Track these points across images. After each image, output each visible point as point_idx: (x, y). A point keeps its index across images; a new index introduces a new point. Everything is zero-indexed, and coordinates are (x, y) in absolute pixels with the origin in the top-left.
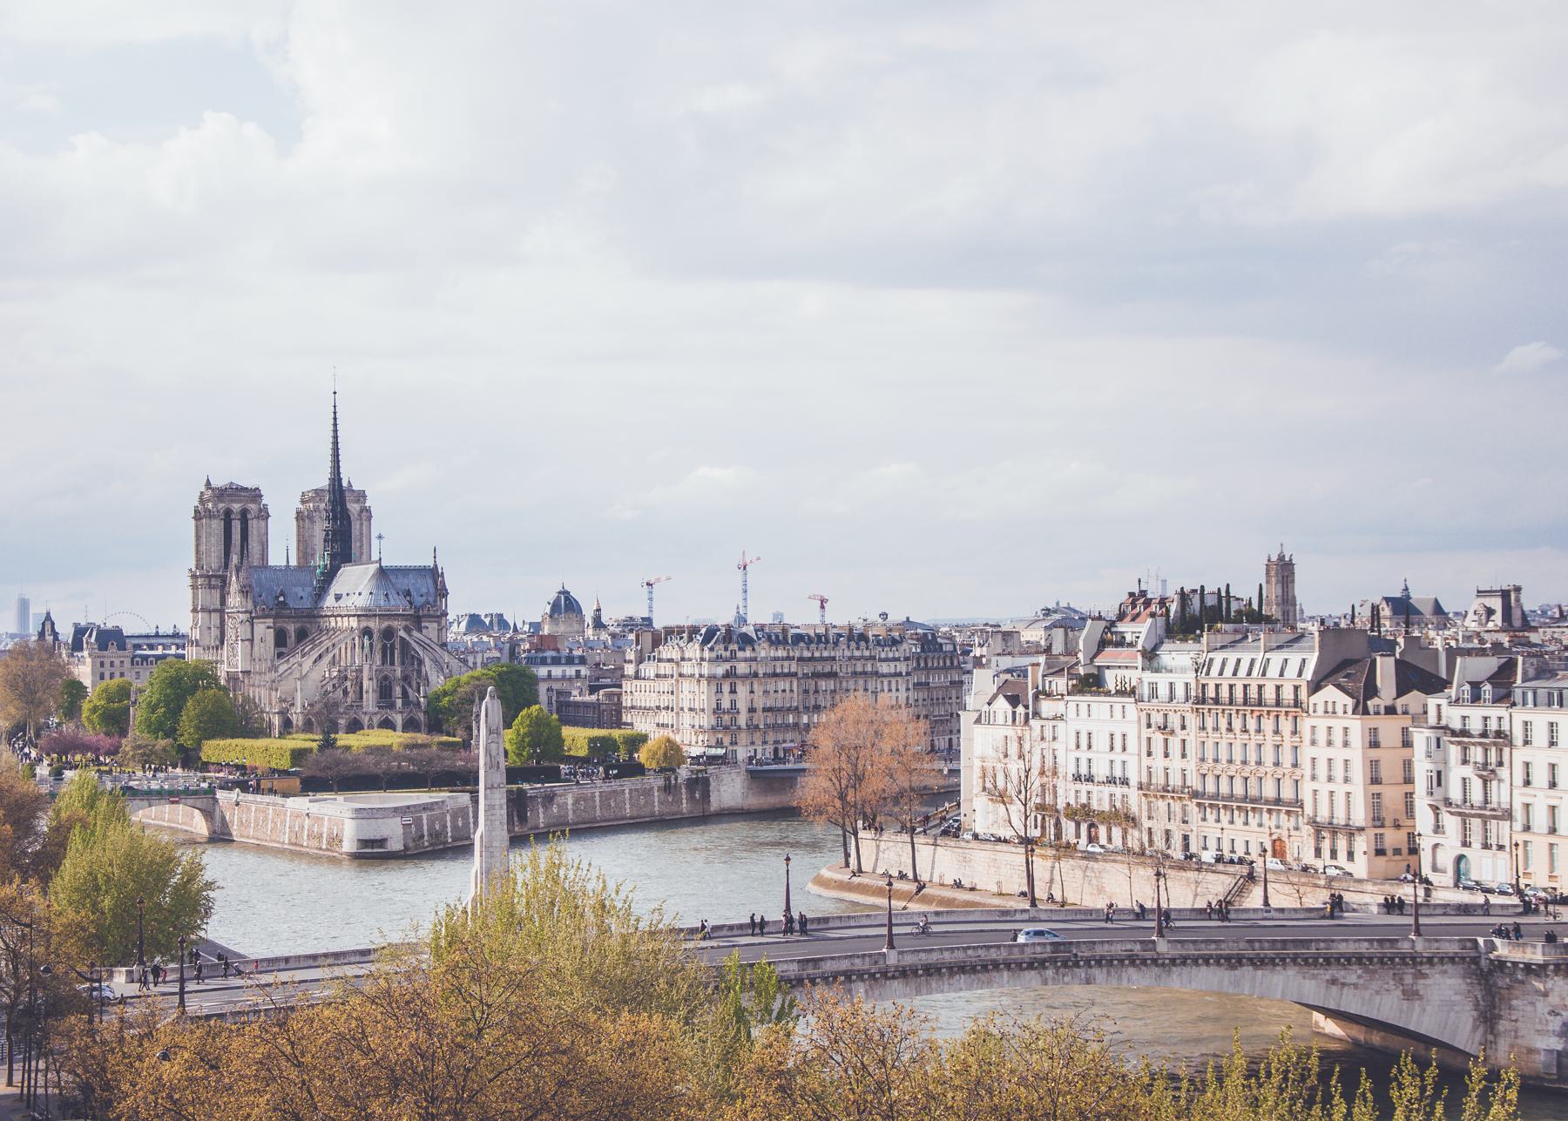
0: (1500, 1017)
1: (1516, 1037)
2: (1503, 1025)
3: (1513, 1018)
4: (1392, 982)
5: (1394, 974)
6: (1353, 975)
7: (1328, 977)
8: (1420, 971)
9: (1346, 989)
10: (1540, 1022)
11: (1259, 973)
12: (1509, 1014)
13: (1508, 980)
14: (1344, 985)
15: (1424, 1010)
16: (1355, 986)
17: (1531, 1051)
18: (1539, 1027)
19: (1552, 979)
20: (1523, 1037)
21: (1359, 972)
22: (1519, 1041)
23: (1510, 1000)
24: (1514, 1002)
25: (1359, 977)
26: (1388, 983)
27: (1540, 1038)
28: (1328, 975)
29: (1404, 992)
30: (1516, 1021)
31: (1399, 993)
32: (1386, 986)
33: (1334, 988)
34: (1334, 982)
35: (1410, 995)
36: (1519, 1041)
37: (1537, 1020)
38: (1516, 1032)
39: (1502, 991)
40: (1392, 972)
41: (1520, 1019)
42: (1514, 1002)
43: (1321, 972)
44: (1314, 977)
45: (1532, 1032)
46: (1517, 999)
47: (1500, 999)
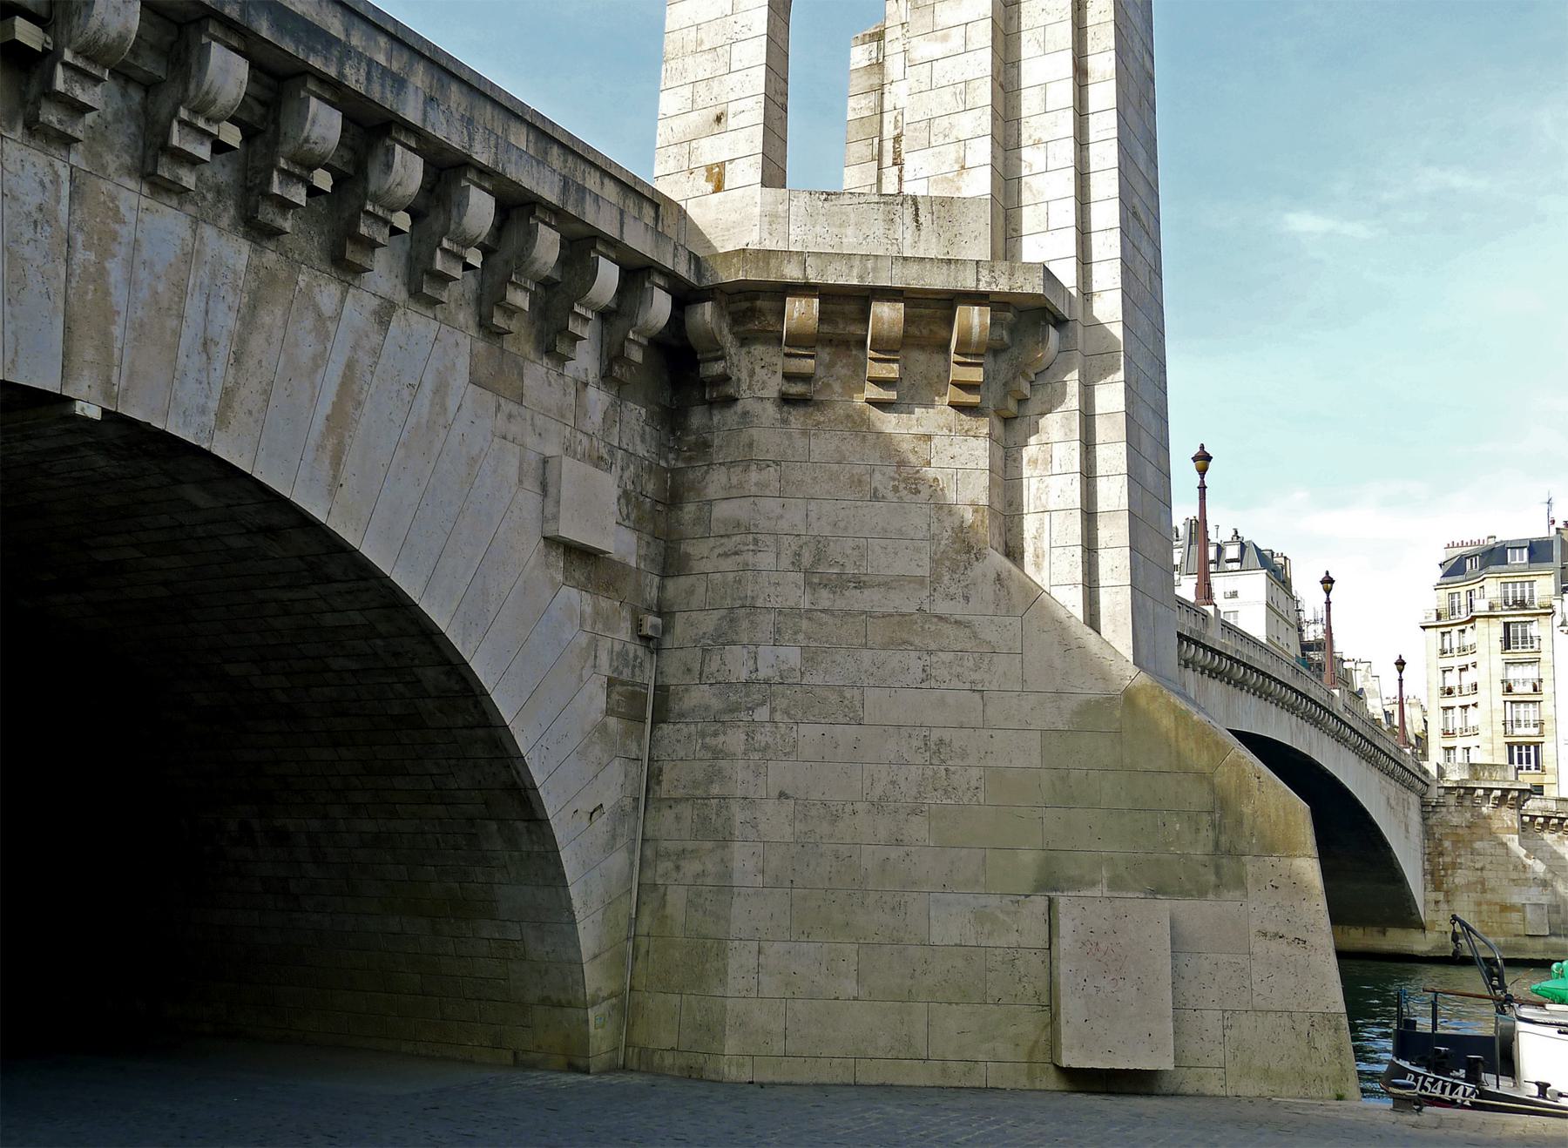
0: (1454, 866)
1: (1484, 891)
2: (1461, 877)
3: (1478, 865)
10: (1516, 868)
12: (1472, 861)
13: (1468, 815)
17: (1505, 908)
18: (1514, 875)
20: (1493, 890)
22: (1489, 896)
23: (1471, 842)
24: (1478, 845)
27: (1516, 889)
30: (1482, 869)
36: (1489, 896)
37: (1511, 867)
38: (1483, 884)
39: (1459, 831)
41: (1488, 866)
42: (1478, 845)
45: (1505, 882)
46: (1481, 839)
47: (1455, 843)
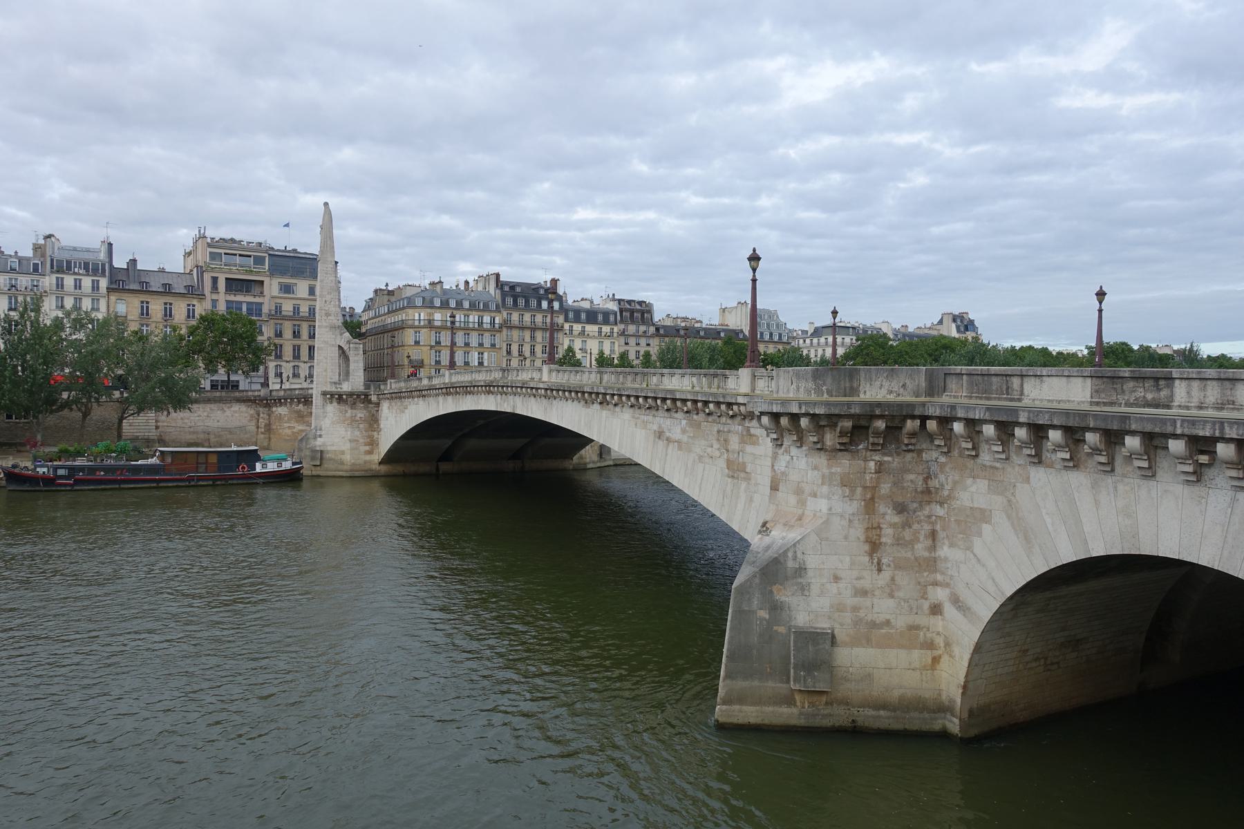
4: (716, 446)
5: (719, 432)
6: (676, 426)
7: (655, 427)
8: (748, 429)
9: (671, 446)
11: (604, 412)
14: (668, 439)
15: (751, 500)
16: (679, 442)
19: (787, 451)
21: (684, 422)
25: (684, 431)
26: (712, 447)
28: (660, 420)
29: (729, 464)
31: (722, 463)
32: (709, 450)
33: (661, 444)
34: (660, 435)
35: (736, 470)
40: (715, 428)
43: (650, 418)
44: (645, 423)
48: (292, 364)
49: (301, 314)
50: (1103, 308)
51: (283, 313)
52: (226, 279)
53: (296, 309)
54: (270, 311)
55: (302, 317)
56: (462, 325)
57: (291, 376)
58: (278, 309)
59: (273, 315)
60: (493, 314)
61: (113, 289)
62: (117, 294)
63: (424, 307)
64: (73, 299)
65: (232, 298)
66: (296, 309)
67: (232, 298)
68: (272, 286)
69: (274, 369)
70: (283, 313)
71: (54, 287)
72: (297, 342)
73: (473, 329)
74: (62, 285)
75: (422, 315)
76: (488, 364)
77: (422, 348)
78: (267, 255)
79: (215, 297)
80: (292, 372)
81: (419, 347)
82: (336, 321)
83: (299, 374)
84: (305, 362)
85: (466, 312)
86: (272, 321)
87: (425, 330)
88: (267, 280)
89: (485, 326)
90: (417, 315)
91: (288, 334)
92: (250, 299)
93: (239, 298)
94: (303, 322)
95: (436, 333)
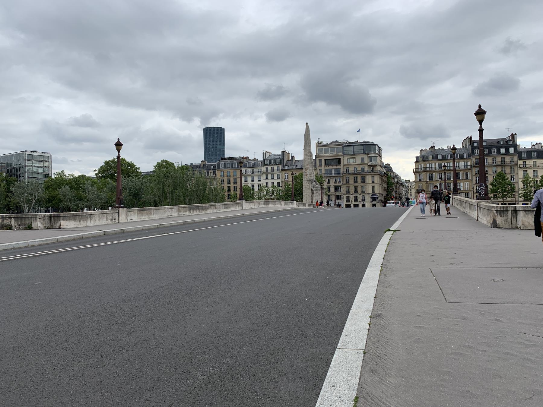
48: (354, 195)
49: (358, 172)
50: (483, 128)
51: (350, 172)
52: (325, 160)
53: (356, 170)
54: (343, 171)
55: (358, 173)
56: (420, 170)
57: (361, 201)
58: (347, 170)
59: (345, 173)
60: (431, 162)
61: (283, 169)
62: (285, 171)
63: (423, 161)
64: (271, 175)
65: (327, 168)
66: (356, 170)
67: (327, 168)
68: (344, 160)
69: (346, 198)
70: (350, 172)
71: (265, 171)
72: (356, 185)
73: (423, 172)
74: (268, 170)
75: (422, 165)
76: (464, 189)
77: (423, 183)
78: (342, 146)
79: (320, 168)
80: (361, 199)
81: (421, 183)
82: (310, 177)
83: (365, 200)
84: (360, 194)
85: (448, 161)
86: (344, 176)
87: (424, 173)
88: (342, 158)
89: (461, 168)
90: (420, 165)
91: (352, 181)
92: (335, 167)
93: (331, 167)
94: (358, 175)
95: (439, 174)
